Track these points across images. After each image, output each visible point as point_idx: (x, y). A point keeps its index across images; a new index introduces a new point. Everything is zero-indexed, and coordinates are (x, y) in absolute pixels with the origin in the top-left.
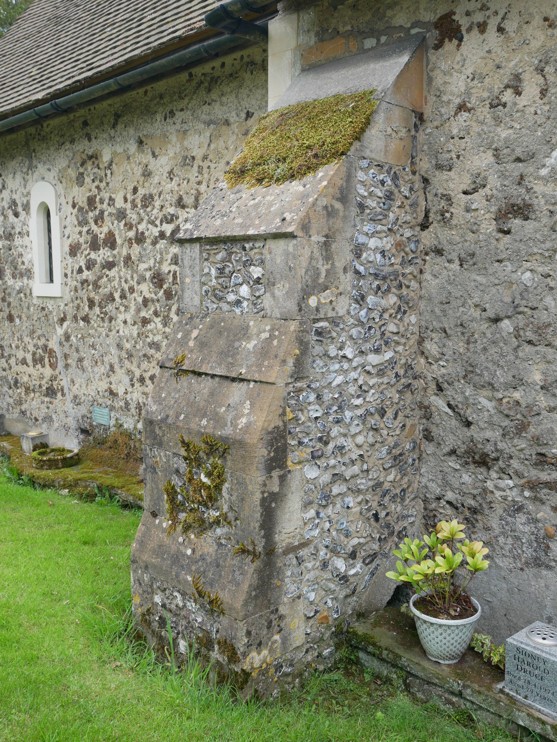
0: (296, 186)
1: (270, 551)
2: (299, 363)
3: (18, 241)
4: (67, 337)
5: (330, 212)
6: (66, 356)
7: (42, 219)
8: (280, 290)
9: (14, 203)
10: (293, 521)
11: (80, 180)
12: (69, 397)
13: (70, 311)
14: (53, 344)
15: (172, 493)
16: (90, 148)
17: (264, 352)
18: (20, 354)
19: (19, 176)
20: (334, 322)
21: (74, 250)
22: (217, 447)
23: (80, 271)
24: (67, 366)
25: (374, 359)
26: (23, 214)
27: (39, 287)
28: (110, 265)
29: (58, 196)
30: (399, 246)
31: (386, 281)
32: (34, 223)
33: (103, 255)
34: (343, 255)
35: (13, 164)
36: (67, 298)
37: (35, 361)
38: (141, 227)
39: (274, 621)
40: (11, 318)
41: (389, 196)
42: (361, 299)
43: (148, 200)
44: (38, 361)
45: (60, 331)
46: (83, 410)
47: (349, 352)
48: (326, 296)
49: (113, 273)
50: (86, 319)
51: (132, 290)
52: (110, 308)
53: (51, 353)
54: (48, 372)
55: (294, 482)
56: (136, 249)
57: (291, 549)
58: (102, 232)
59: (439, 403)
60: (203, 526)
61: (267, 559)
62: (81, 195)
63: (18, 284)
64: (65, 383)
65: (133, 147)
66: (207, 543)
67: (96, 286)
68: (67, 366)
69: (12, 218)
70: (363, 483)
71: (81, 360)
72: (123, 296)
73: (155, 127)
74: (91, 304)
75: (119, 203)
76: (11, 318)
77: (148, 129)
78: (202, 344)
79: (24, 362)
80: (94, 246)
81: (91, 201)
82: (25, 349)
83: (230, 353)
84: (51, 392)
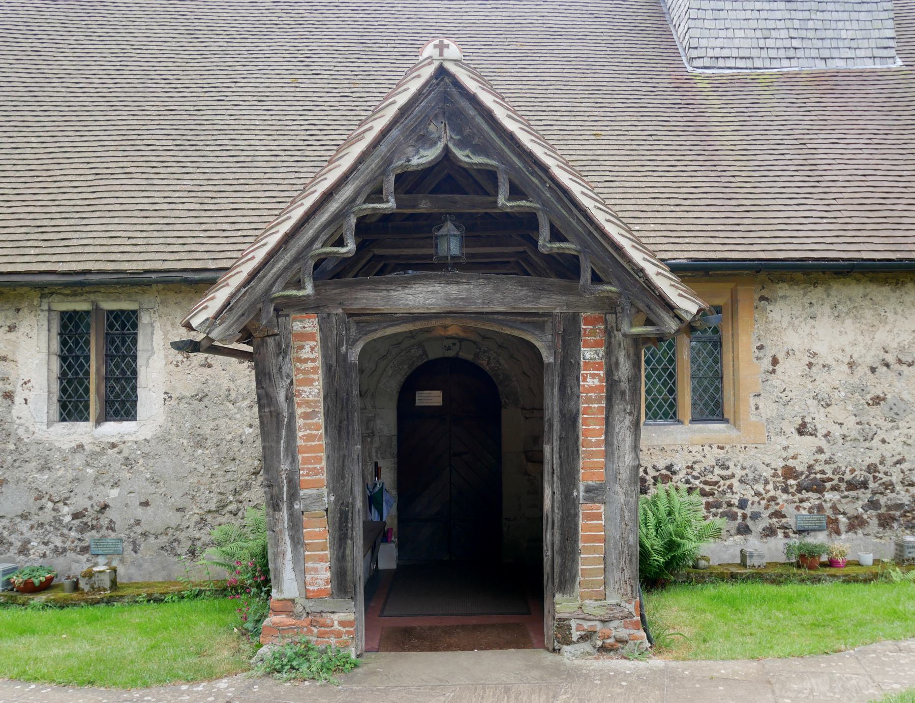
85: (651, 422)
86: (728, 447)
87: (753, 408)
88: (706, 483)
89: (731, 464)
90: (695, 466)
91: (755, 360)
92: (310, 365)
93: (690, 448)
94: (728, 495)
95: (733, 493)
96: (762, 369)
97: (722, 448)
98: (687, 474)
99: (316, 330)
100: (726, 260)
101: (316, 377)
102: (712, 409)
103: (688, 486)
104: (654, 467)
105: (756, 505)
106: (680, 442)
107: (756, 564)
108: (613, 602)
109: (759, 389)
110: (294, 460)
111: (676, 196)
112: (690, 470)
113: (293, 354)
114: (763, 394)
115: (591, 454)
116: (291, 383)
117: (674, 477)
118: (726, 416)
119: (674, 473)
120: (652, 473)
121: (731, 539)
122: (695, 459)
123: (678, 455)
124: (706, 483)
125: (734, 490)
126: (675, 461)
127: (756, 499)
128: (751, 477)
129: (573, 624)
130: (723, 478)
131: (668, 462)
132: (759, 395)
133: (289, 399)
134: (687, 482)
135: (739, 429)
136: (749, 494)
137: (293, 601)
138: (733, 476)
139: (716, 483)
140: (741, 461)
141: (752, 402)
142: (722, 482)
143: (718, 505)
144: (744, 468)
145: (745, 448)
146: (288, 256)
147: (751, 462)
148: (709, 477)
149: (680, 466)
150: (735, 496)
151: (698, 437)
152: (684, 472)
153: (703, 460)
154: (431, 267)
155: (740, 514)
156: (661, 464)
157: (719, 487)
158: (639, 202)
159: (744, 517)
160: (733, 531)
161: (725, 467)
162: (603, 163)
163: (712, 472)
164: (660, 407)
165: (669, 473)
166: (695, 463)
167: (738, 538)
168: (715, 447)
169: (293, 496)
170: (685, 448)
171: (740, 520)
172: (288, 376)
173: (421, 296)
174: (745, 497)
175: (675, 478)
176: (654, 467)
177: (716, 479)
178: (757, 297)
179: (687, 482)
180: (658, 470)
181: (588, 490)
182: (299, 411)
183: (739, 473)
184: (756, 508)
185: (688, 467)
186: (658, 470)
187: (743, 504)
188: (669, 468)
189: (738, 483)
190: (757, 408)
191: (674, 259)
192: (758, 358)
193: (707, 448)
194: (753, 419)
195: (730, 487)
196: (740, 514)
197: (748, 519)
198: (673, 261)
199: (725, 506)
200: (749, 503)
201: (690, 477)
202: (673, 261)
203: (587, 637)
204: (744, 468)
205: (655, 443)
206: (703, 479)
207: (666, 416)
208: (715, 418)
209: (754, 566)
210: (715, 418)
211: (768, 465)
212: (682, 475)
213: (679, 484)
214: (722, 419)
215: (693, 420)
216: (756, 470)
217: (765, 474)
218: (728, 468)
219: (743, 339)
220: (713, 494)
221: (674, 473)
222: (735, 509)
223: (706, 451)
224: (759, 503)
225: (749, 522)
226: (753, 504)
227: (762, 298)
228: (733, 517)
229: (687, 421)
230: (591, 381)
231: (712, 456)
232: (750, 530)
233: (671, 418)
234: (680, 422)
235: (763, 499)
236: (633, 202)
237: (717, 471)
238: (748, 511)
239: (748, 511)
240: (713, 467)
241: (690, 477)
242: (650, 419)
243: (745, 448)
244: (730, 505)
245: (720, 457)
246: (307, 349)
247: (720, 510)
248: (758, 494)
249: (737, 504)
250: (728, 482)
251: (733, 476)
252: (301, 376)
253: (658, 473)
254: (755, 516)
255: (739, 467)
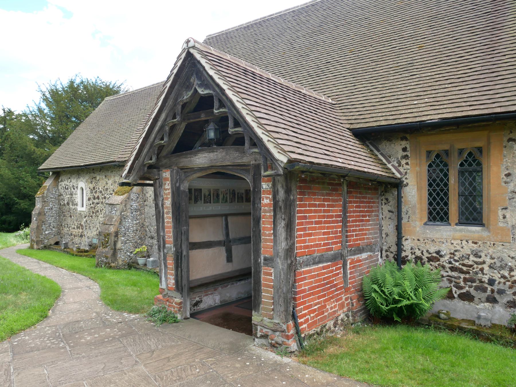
0: (122, 197)
1: (115, 249)
2: (120, 222)
3: (74, 196)
4: (86, 221)
5: (126, 201)
6: (86, 226)
7: (81, 191)
8: (118, 212)
9: (74, 186)
10: (119, 245)
11: (91, 182)
12: (86, 237)
13: (88, 214)
14: (83, 223)
15: (102, 243)
16: (95, 175)
17: (116, 221)
18: (73, 226)
19: (75, 179)
20: (127, 216)
21: (89, 199)
22: (109, 234)
23: (91, 204)
24: (86, 229)
25: (135, 222)
26: (76, 189)
27: (79, 208)
28: (98, 204)
29: (86, 186)
30: (140, 205)
31: (136, 210)
32: (79, 192)
33: (96, 201)
34: (128, 206)
35: (74, 176)
36: (87, 211)
37: (77, 228)
38: (105, 195)
39: (116, 260)
40: (71, 216)
41: (138, 197)
42: (132, 213)
43: (107, 189)
44: (78, 228)
45: (85, 220)
46: (90, 240)
47: (130, 221)
48: (125, 213)
49: (98, 205)
50: (91, 216)
51: (103, 209)
52: (97, 214)
53: (82, 225)
54: (81, 230)
55: (120, 239)
56: (104, 200)
57: (119, 249)
58: (96, 195)
59: (147, 229)
60: (107, 247)
61: (115, 251)
62: (91, 186)
63: (73, 207)
64: (85, 233)
65: (104, 177)
66: (107, 249)
67: (94, 208)
68: (86, 229)
69: (73, 190)
70: (133, 241)
71: (90, 227)
72: (101, 211)
73: (109, 173)
74: (93, 213)
75: (101, 189)
76: (71, 216)
77: (107, 174)
78: (108, 220)
79: (74, 228)
80: (94, 199)
81: (94, 188)
82: (75, 225)
83: (111, 221)
84: (81, 236)
85: (431, 223)
86: (480, 243)
87: (501, 217)
88: (463, 265)
89: (483, 255)
90: (456, 253)
91: (503, 184)
92: (168, 191)
93: (452, 242)
94: (479, 275)
95: (483, 274)
96: (509, 190)
97: (476, 243)
98: (450, 258)
99: (169, 176)
100: (468, 116)
101: (169, 196)
102: (473, 215)
103: (451, 265)
104: (427, 251)
105: (501, 285)
106: (445, 237)
107: (483, 324)
108: (277, 321)
109: (507, 203)
110: (164, 232)
111: (453, 77)
112: (452, 256)
113: (163, 187)
114: (509, 208)
115: (266, 241)
116: (163, 199)
117: (441, 259)
118: (484, 222)
119: (441, 256)
120: (426, 255)
121: (482, 304)
122: (456, 249)
123: (444, 245)
124: (463, 265)
125: (485, 272)
126: (442, 249)
127: (502, 280)
128: (498, 264)
129: (259, 328)
130: (476, 263)
131: (437, 249)
132: (506, 209)
133: (162, 205)
134: (450, 263)
135: (489, 232)
136: (496, 276)
137: (164, 289)
138: (484, 263)
139: (471, 266)
140: (489, 253)
141: (500, 213)
142: (475, 266)
143: (473, 281)
144: (492, 258)
145: (494, 244)
146: (147, 146)
147: (499, 254)
148: (466, 262)
149: (445, 252)
150: (484, 276)
151: (458, 235)
152: (449, 256)
153: (461, 250)
154: (208, 145)
155: (489, 289)
156: (432, 250)
157: (473, 269)
158: (425, 85)
159: (493, 291)
160: (483, 299)
161: (477, 255)
162: (415, 64)
163: (468, 259)
164: (438, 213)
165: (438, 256)
166: (456, 251)
167: (487, 305)
168: (470, 242)
169: (164, 247)
170: (449, 241)
171: (489, 292)
172: (162, 196)
173: (202, 159)
174: (494, 278)
175: (442, 259)
176: (427, 251)
177: (470, 263)
178: (505, 139)
179: (450, 263)
180: (430, 254)
181: (265, 259)
182: (165, 211)
183: (488, 261)
184: (501, 287)
185: (451, 254)
186: (430, 254)
187: (491, 282)
188: (438, 252)
189: (488, 268)
190: (504, 217)
191: (431, 120)
192: (506, 183)
193: (464, 242)
194: (501, 225)
195: (482, 270)
196: (489, 289)
197: (496, 293)
198: (430, 121)
199: (478, 282)
200: (497, 282)
201: (452, 260)
202: (430, 121)
203: (265, 336)
204: (492, 258)
205: (429, 236)
206: (461, 262)
207: (442, 219)
208: (469, 222)
209: (480, 325)
210: (469, 222)
211: (512, 258)
212: (447, 258)
213: (444, 264)
214: (482, 225)
215: (460, 223)
216: (502, 260)
217: (510, 264)
218: (480, 257)
219: (494, 169)
220: (469, 273)
221: (441, 256)
222: (486, 285)
223: (463, 245)
224: (504, 283)
225: (497, 296)
226: (499, 283)
227: (510, 140)
228: (485, 290)
229: (453, 224)
230: (266, 200)
231: (468, 248)
232: (497, 301)
233: (445, 221)
234: (450, 224)
235: (509, 281)
236: (421, 86)
237: (472, 258)
238: (496, 288)
239: (496, 288)
240: (469, 255)
241: (452, 260)
242: (431, 221)
243: (494, 244)
244: (481, 281)
245: (474, 249)
246: (167, 185)
247: (474, 284)
248: (503, 277)
249: (487, 281)
250: (480, 267)
251: (484, 263)
252: (165, 196)
253: (430, 255)
254: (501, 292)
255: (489, 257)
